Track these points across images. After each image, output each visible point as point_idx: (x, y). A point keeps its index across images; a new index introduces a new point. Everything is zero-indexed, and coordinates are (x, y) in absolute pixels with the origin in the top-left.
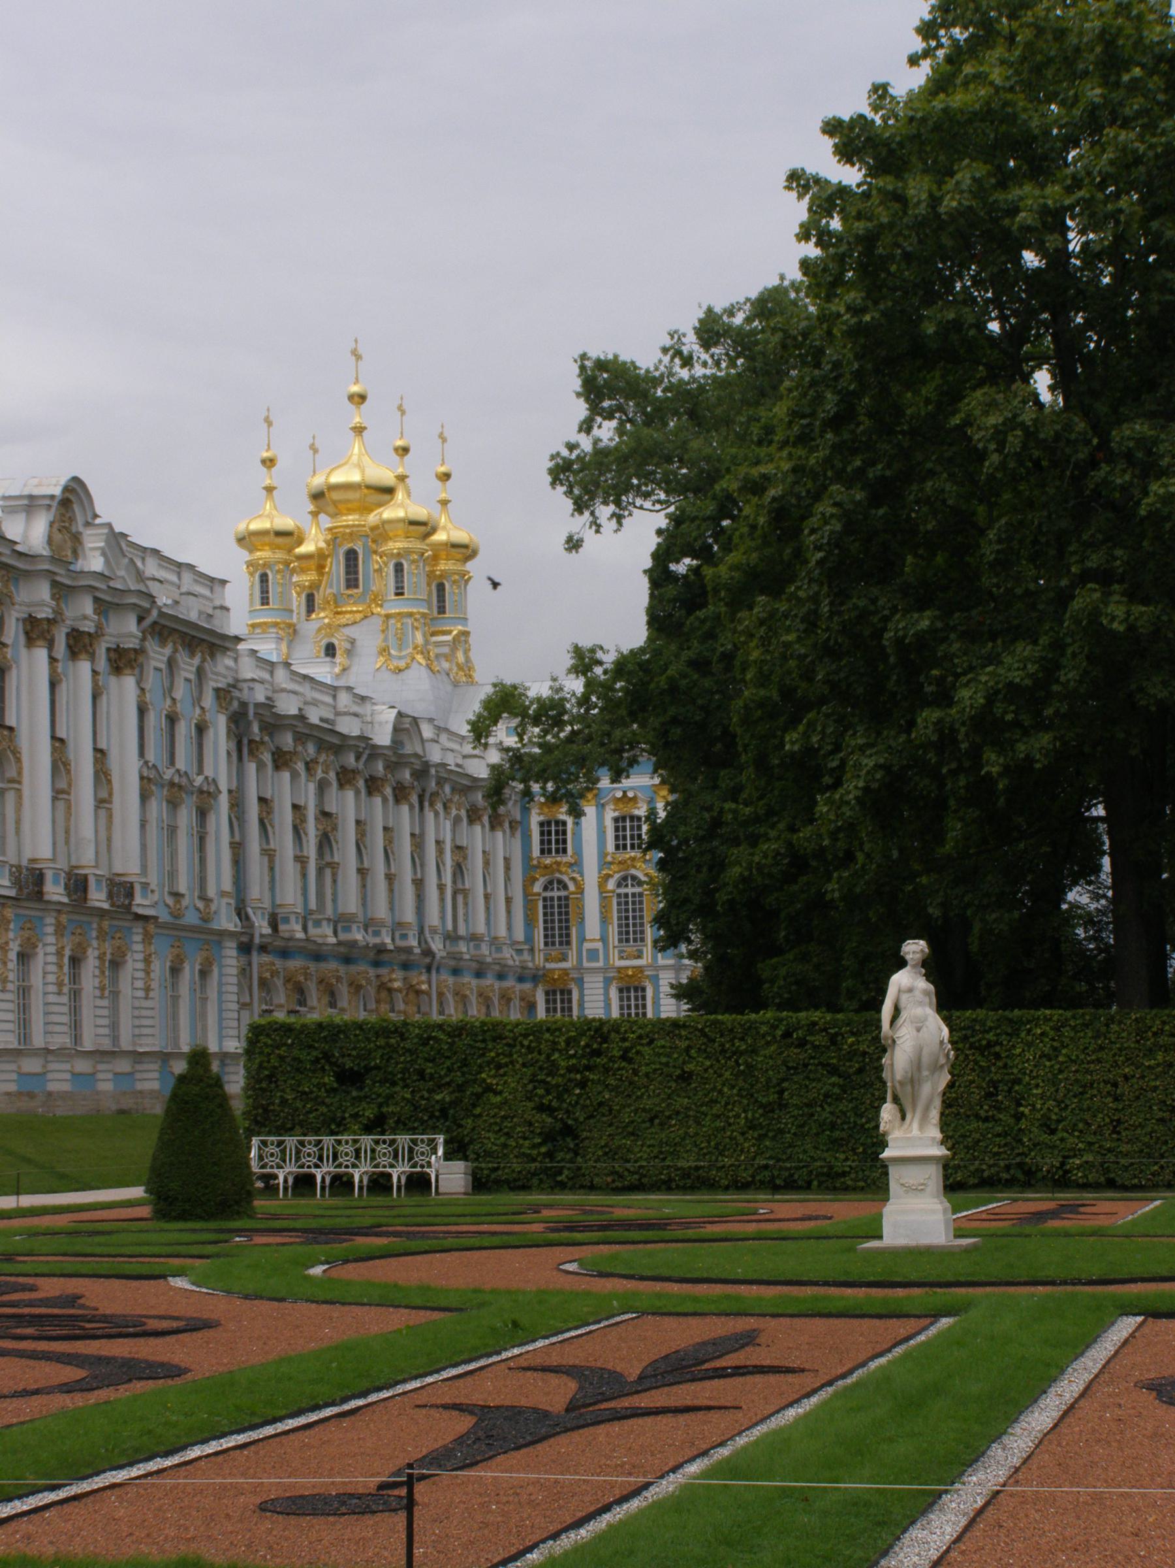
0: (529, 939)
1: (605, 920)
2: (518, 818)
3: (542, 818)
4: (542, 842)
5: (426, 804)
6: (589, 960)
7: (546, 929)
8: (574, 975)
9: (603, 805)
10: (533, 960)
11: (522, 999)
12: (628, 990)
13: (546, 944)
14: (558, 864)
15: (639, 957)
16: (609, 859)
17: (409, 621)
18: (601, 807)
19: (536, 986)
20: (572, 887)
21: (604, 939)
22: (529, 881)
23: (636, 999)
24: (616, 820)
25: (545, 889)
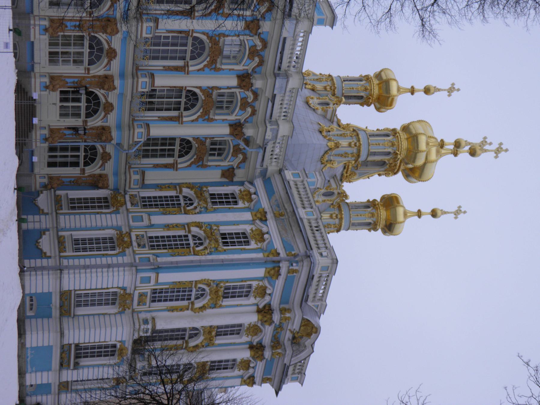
1: (168, 227)
11: (100, 176)
15: (139, 245)
21: (151, 226)
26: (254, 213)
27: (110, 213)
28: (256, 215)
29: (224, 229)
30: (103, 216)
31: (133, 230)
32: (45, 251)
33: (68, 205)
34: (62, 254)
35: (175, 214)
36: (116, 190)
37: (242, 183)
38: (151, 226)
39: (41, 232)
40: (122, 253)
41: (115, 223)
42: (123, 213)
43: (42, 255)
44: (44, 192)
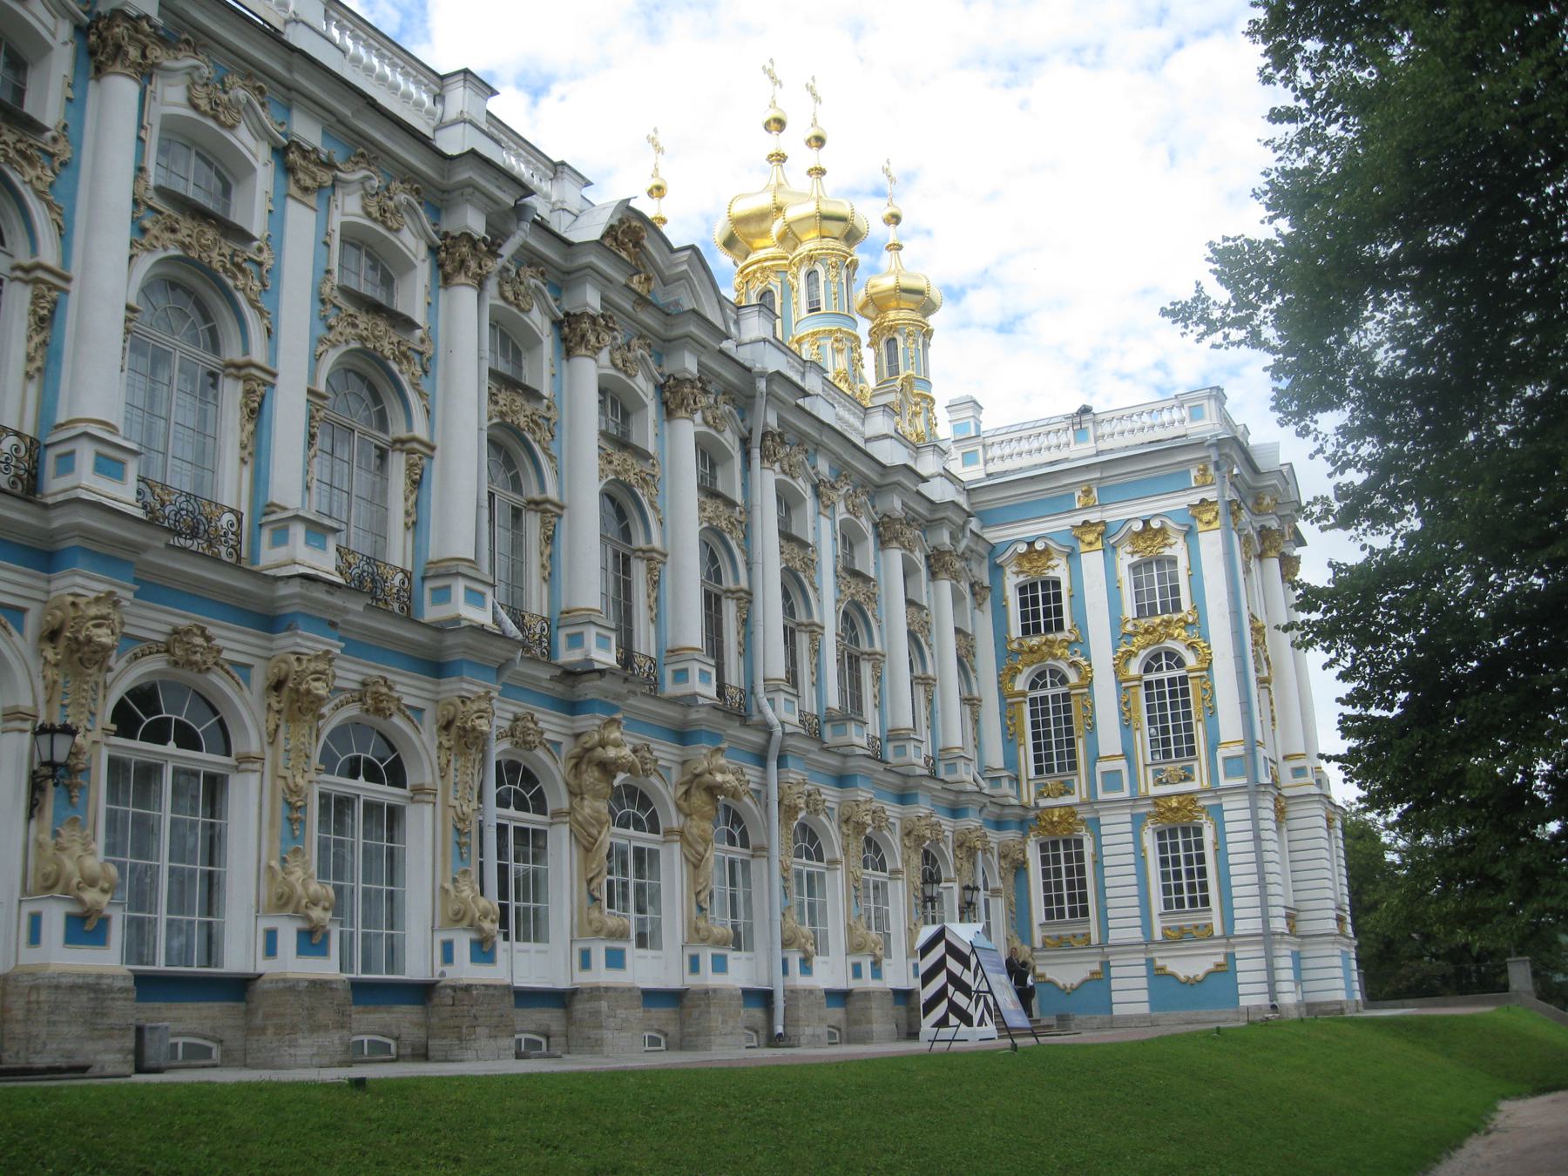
0: (1011, 762)
2: (986, 583)
3: (1022, 578)
4: (1024, 616)
5: (756, 453)
6: (1105, 790)
7: (1037, 747)
8: (1083, 813)
9: (1114, 548)
10: (1019, 795)
11: (1003, 856)
12: (1173, 833)
13: (1039, 770)
14: (1049, 644)
15: (1187, 778)
16: (1129, 628)
17: (828, 343)
18: (1110, 551)
19: (1025, 836)
20: (1073, 678)
21: (1128, 755)
22: (1007, 674)
23: (1187, 847)
24: (1135, 568)
25: (1033, 686)
26: (1083, 548)
27: (1097, 837)
28: (1090, 544)
29: (1129, 610)
30: (1105, 851)
31: (1143, 790)
32: (1211, 967)
33: (1067, 923)
34: (1217, 931)
35: (1093, 706)
36: (1023, 824)
37: (997, 569)
38: (1128, 755)
39: (1158, 975)
40: (1217, 813)
41: (1129, 827)
42: (1097, 811)
43: (1226, 971)
44: (1039, 970)
